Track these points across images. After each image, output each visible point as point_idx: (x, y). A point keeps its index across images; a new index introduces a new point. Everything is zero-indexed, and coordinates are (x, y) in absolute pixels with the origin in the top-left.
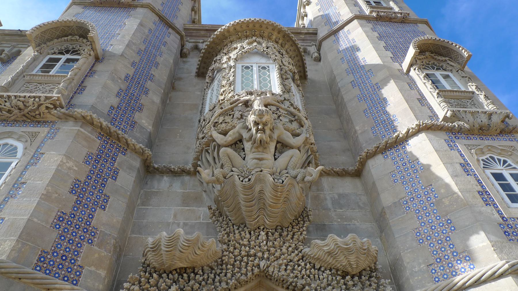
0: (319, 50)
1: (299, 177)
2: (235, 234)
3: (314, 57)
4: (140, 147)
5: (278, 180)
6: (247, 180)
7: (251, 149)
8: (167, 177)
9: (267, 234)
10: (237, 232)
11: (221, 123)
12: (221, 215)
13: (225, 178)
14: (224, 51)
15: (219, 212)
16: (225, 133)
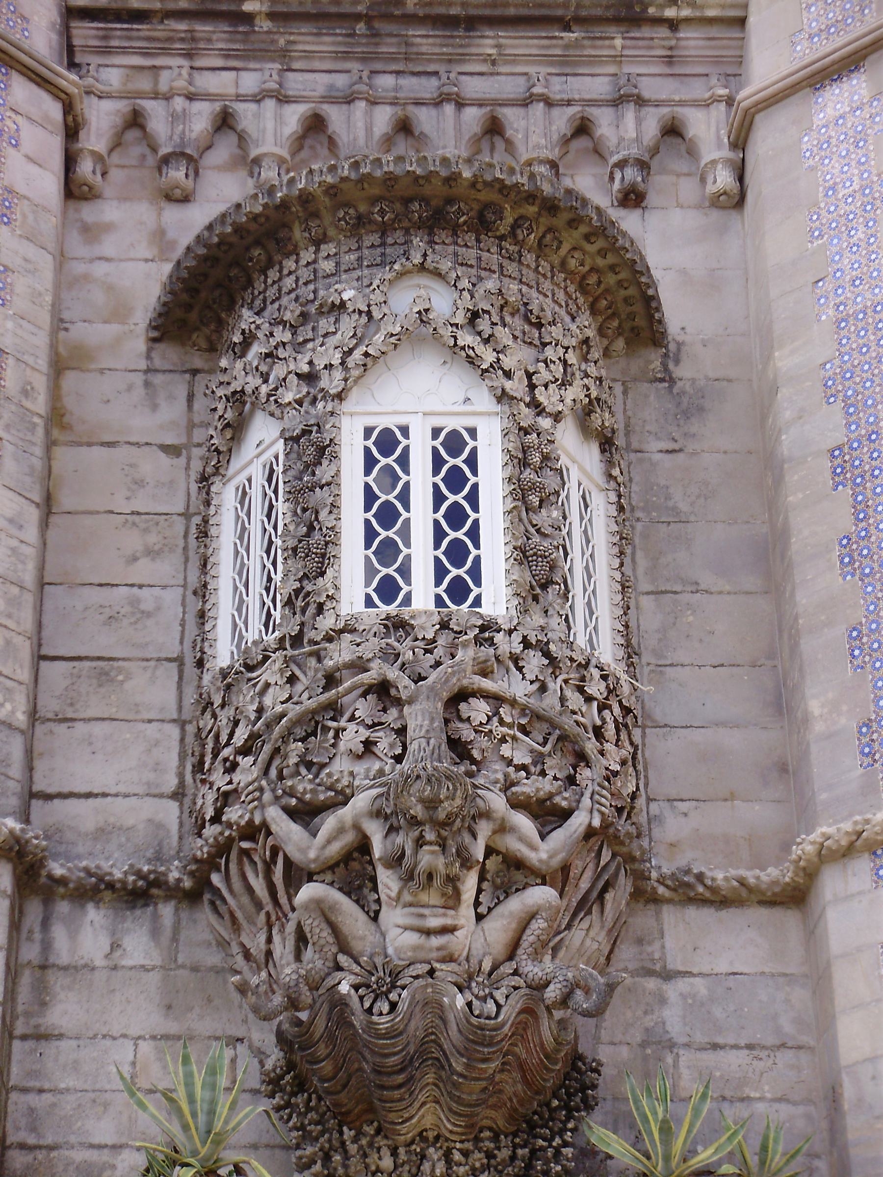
0: (740, 141)
1: (552, 993)
2: (346, 1151)
3: (711, 189)
4: (11, 832)
5: (484, 999)
6: (386, 1008)
7: (400, 893)
8: (98, 908)
9: (447, 1155)
10: (353, 1148)
11: (297, 765)
12: (301, 1085)
13: (314, 987)
14: (288, 316)
15: (294, 1078)
16: (306, 814)
